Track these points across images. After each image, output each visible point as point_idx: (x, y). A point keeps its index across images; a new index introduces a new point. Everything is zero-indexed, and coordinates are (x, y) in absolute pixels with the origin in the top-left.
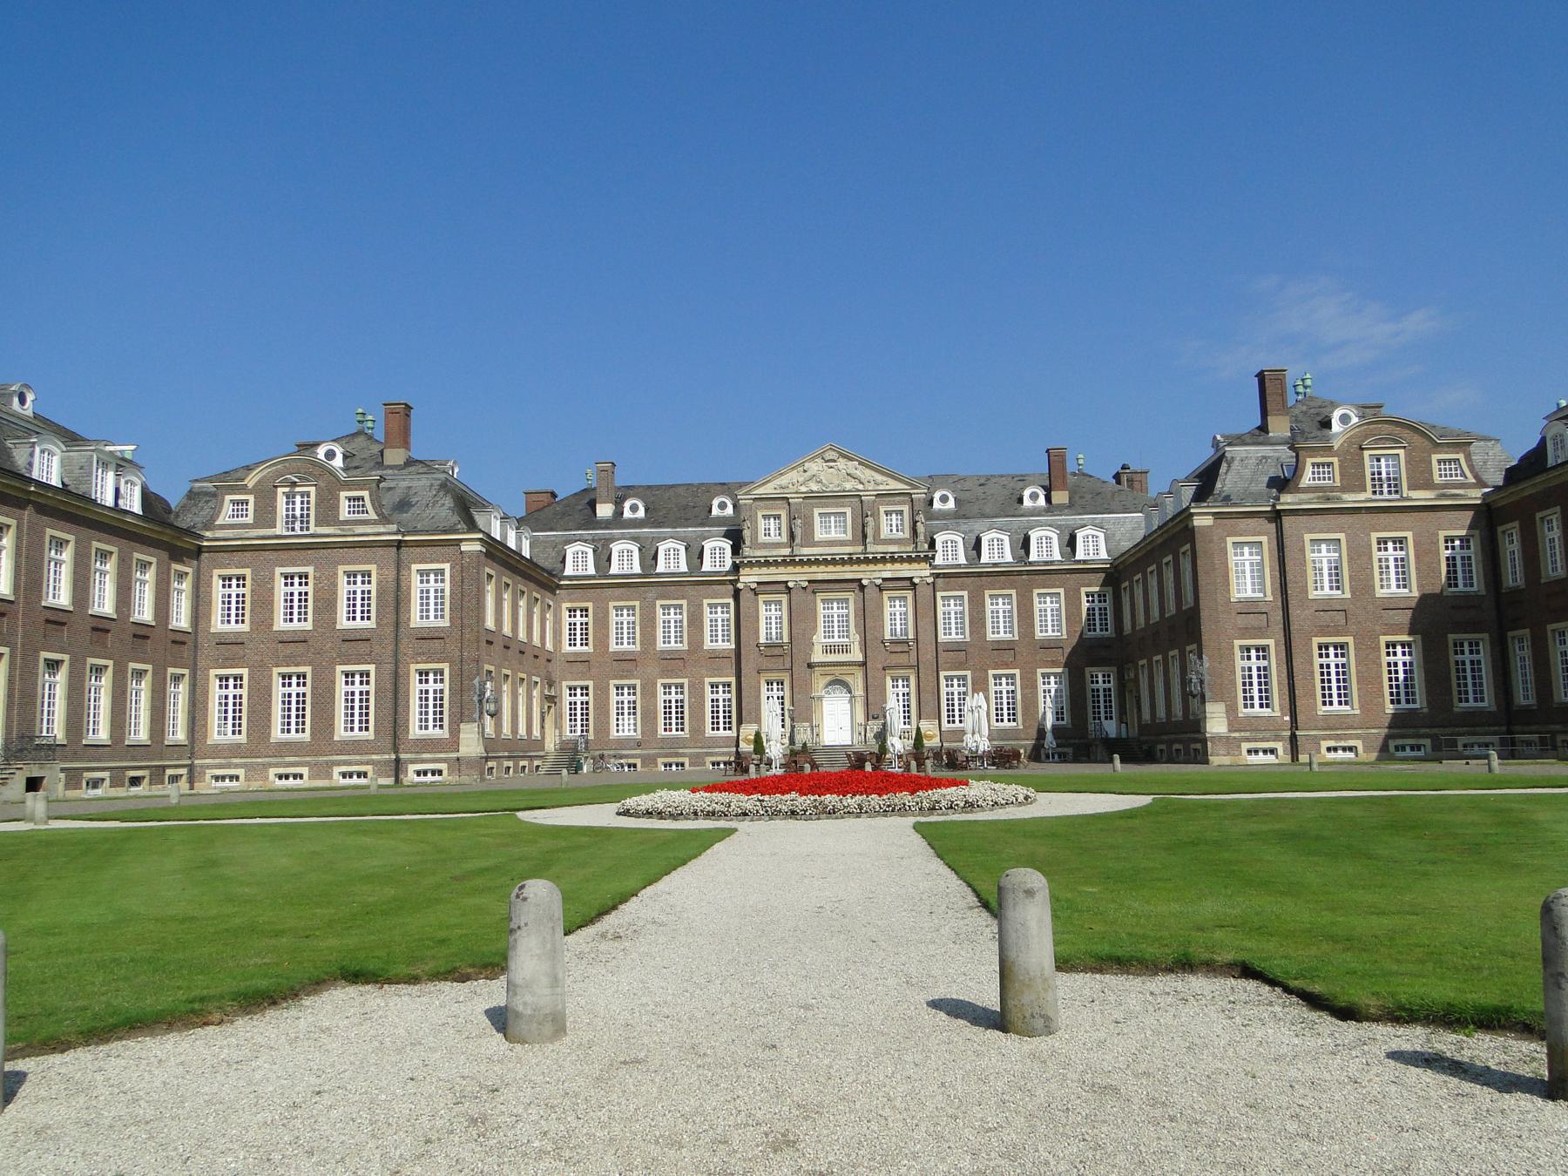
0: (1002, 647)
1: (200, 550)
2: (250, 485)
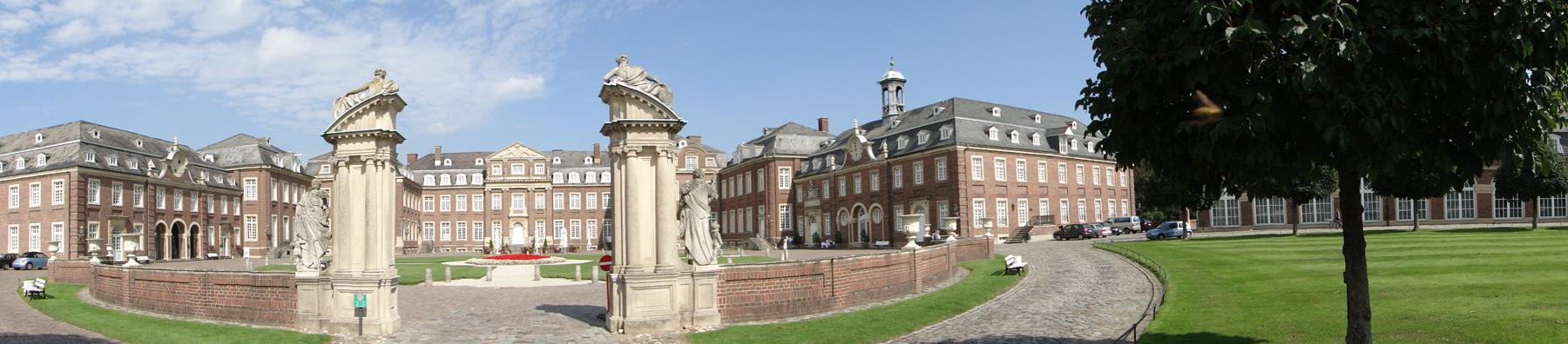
0: (575, 212)
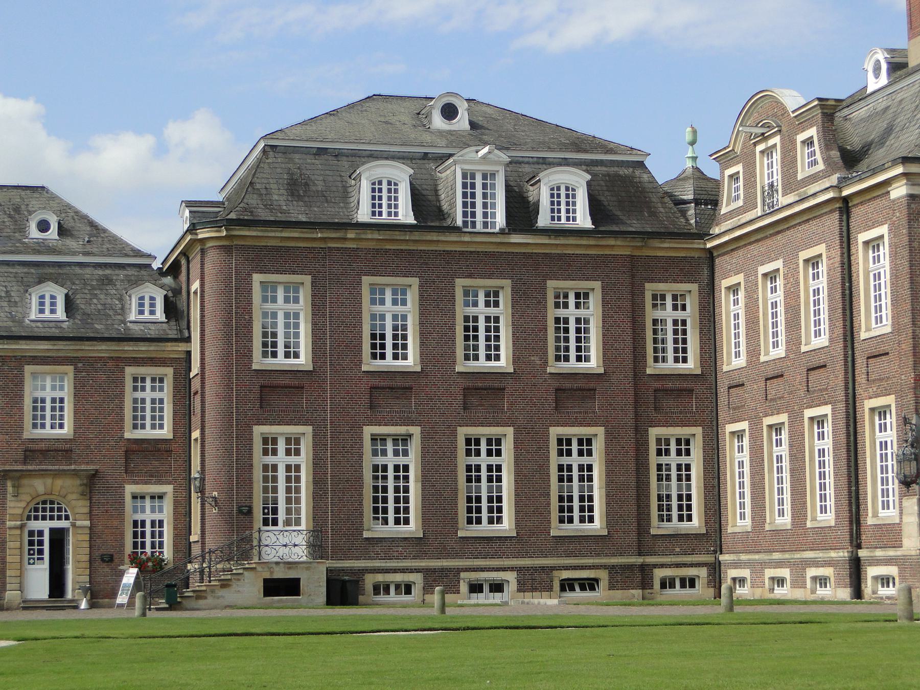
1: (711, 256)
2: (738, 150)
